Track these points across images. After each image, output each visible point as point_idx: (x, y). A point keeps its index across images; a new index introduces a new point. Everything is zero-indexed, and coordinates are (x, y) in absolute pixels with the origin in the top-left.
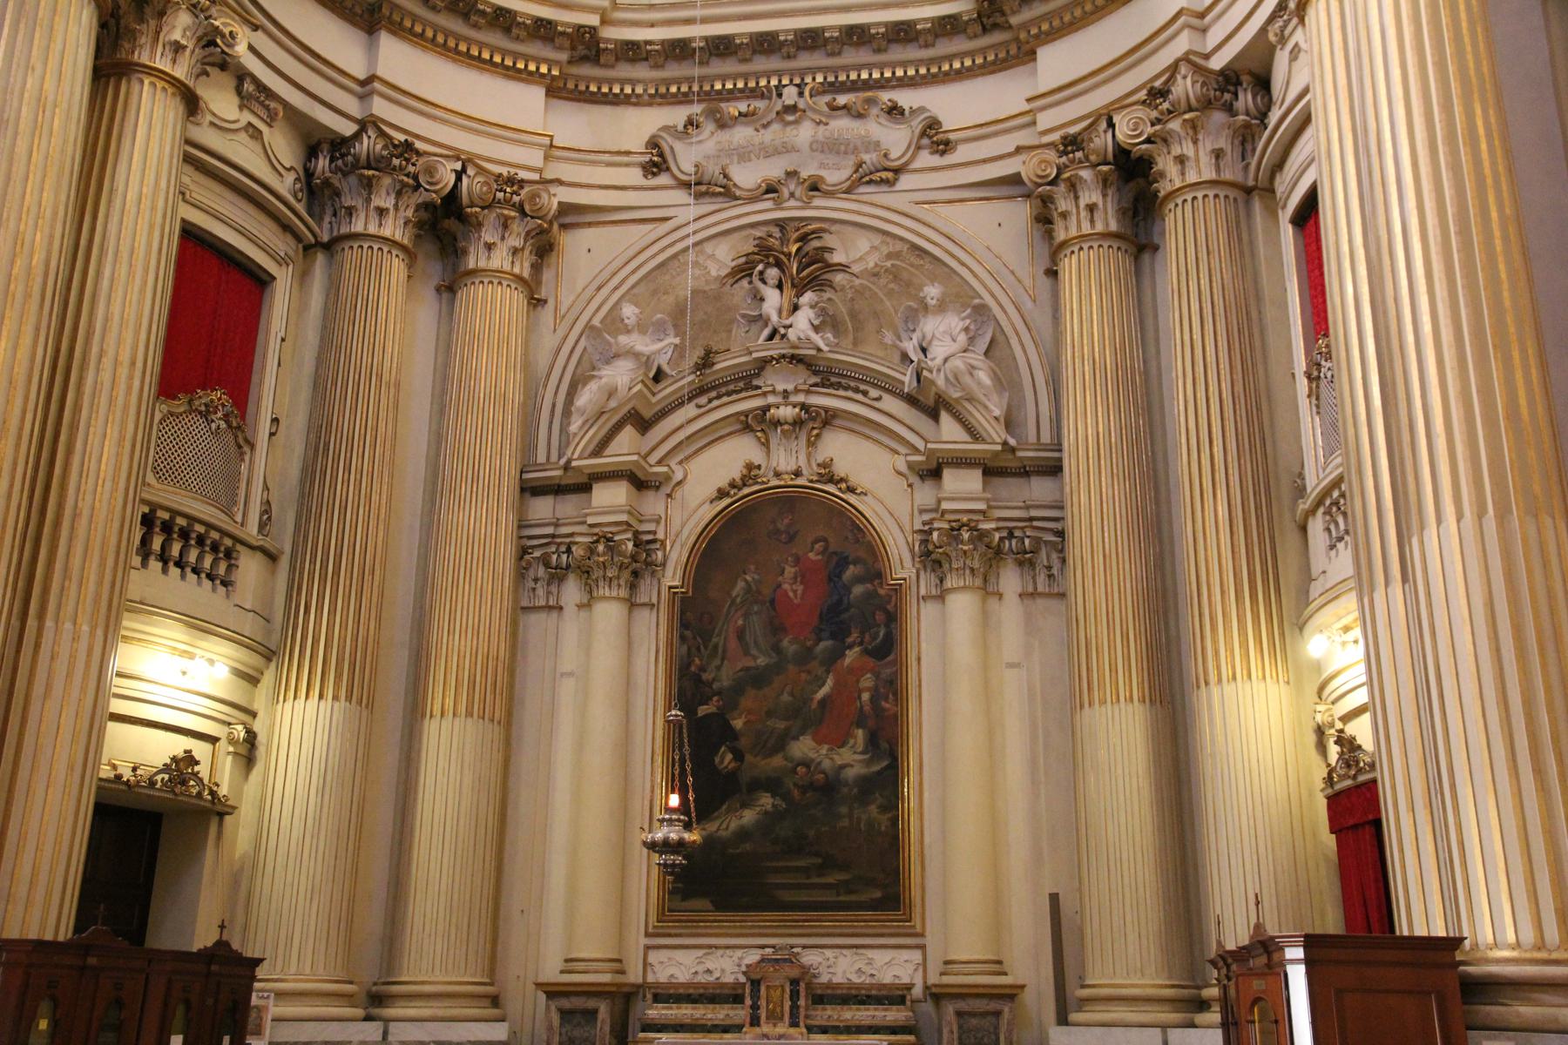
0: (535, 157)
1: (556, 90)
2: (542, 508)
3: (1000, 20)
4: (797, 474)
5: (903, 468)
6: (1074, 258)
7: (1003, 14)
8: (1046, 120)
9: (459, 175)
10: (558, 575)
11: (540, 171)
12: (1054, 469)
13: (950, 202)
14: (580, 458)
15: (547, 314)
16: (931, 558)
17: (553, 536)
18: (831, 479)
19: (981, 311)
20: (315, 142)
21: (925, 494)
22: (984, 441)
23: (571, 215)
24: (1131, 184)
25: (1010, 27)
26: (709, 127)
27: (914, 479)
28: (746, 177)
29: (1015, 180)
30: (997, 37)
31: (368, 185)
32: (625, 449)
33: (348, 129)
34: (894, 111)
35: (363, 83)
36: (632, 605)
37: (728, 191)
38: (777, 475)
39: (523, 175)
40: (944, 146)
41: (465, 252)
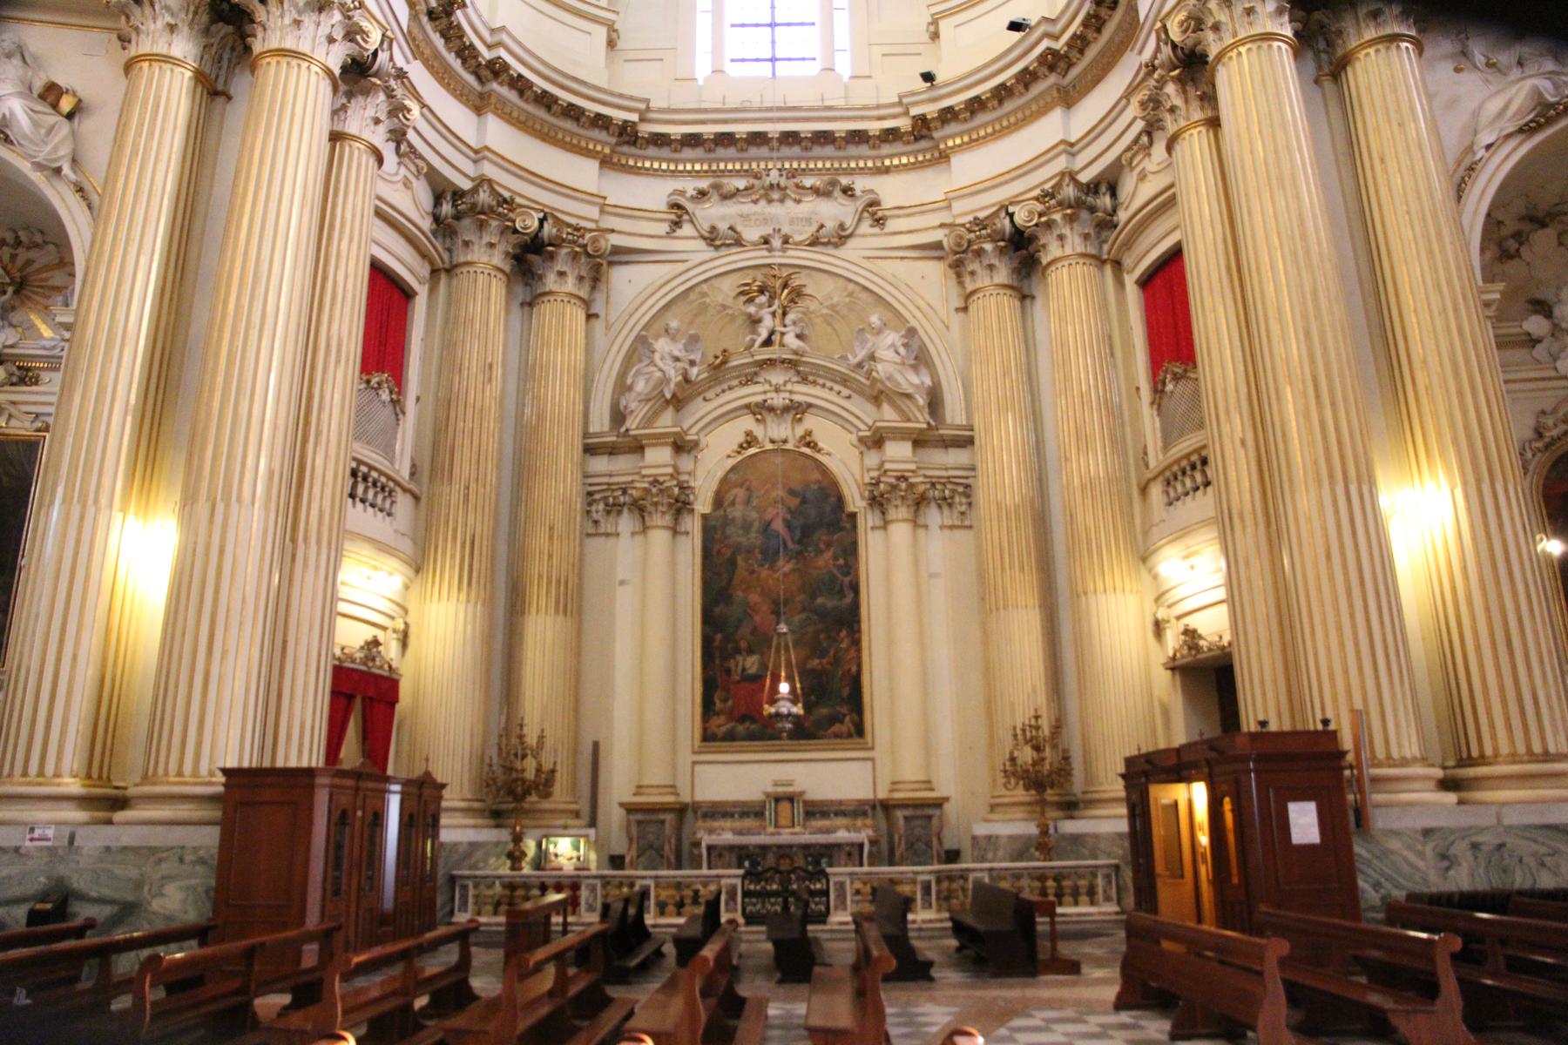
0: (594, 212)
1: (606, 163)
2: (600, 464)
3: (925, 132)
4: (785, 441)
5: (855, 442)
6: (980, 301)
7: (929, 129)
8: (958, 207)
9: (541, 221)
10: (614, 509)
11: (596, 222)
12: (967, 442)
13: (902, 258)
14: (637, 428)
15: (598, 325)
16: (878, 502)
17: (609, 484)
18: (808, 445)
19: (912, 332)
20: (441, 190)
21: (872, 459)
22: (909, 420)
23: (621, 256)
24: (1019, 253)
25: (932, 138)
26: (715, 198)
27: (863, 449)
28: (751, 234)
29: (938, 246)
30: (924, 144)
31: (482, 226)
32: (666, 422)
33: (466, 185)
34: (847, 191)
35: (476, 152)
36: (675, 531)
37: (739, 242)
38: (772, 441)
39: (583, 224)
40: (879, 221)
41: (541, 278)
